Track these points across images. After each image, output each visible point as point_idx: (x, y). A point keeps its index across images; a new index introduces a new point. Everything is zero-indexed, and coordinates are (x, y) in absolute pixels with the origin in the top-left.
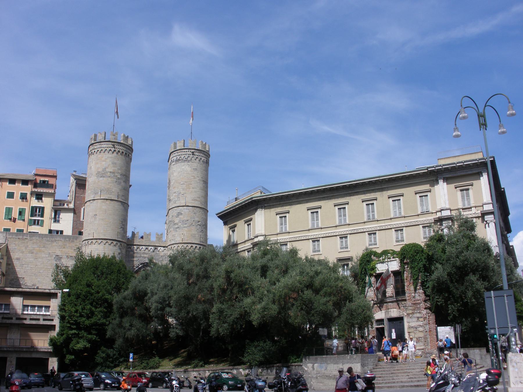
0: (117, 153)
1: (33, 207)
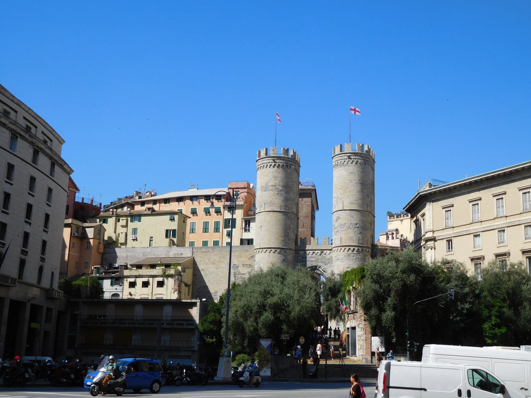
0: (278, 167)
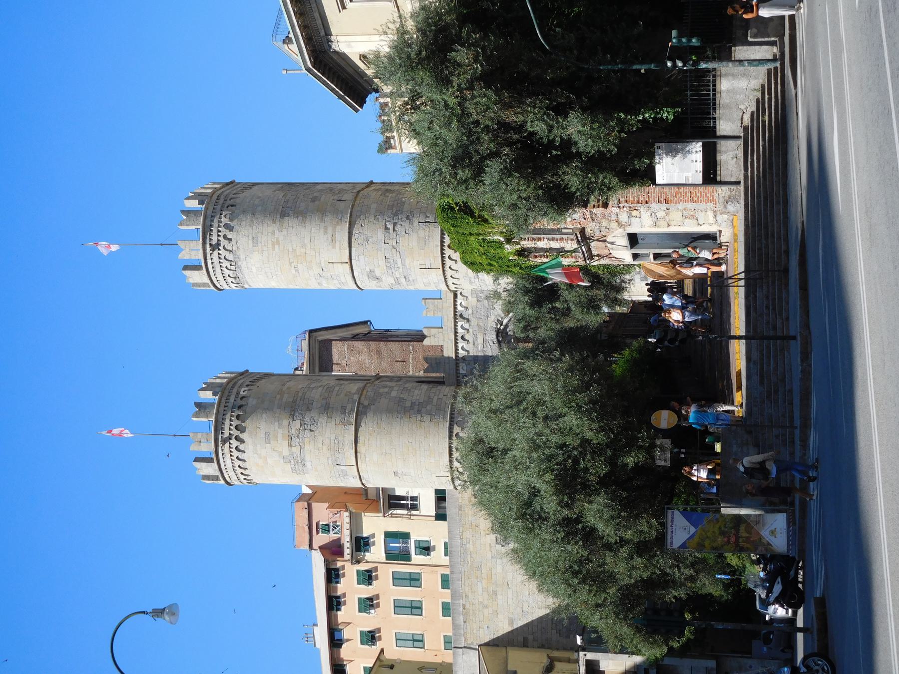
0: (243, 431)
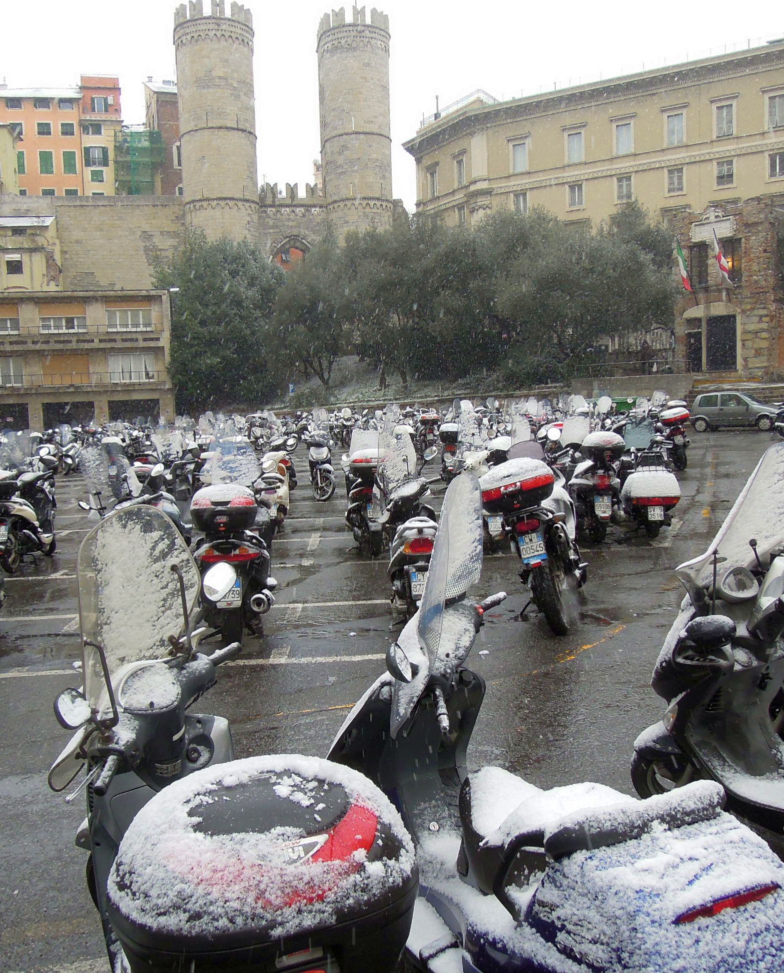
1: (87, 150)
